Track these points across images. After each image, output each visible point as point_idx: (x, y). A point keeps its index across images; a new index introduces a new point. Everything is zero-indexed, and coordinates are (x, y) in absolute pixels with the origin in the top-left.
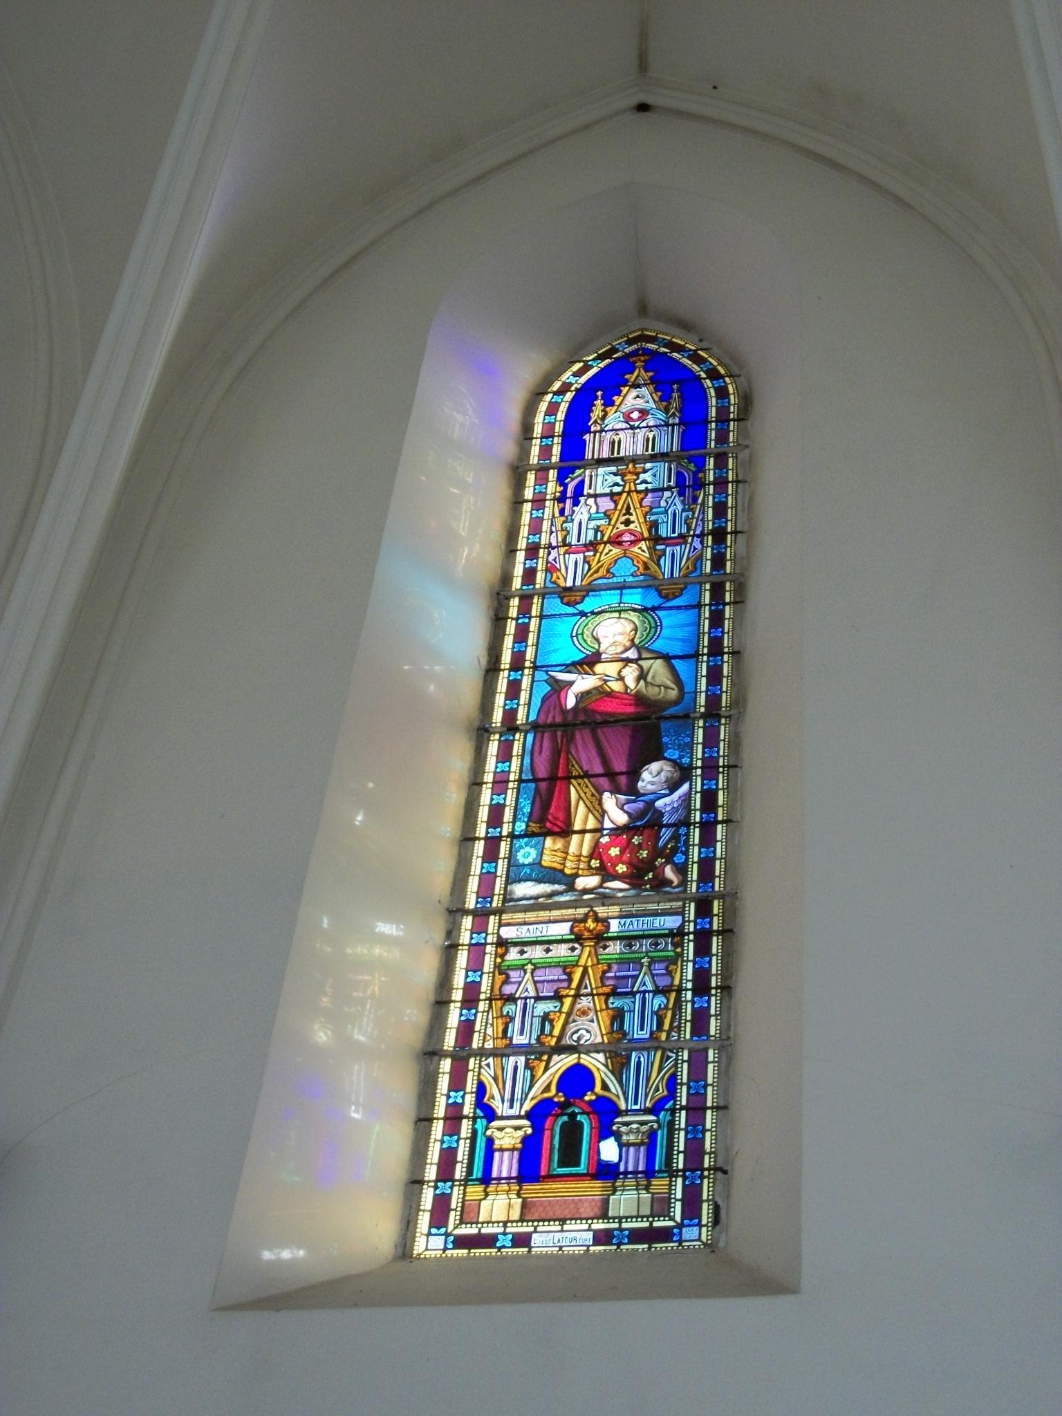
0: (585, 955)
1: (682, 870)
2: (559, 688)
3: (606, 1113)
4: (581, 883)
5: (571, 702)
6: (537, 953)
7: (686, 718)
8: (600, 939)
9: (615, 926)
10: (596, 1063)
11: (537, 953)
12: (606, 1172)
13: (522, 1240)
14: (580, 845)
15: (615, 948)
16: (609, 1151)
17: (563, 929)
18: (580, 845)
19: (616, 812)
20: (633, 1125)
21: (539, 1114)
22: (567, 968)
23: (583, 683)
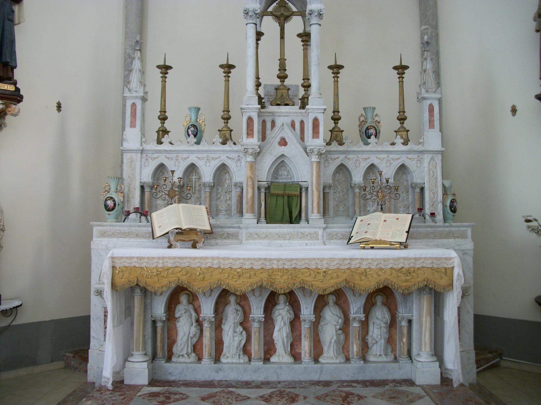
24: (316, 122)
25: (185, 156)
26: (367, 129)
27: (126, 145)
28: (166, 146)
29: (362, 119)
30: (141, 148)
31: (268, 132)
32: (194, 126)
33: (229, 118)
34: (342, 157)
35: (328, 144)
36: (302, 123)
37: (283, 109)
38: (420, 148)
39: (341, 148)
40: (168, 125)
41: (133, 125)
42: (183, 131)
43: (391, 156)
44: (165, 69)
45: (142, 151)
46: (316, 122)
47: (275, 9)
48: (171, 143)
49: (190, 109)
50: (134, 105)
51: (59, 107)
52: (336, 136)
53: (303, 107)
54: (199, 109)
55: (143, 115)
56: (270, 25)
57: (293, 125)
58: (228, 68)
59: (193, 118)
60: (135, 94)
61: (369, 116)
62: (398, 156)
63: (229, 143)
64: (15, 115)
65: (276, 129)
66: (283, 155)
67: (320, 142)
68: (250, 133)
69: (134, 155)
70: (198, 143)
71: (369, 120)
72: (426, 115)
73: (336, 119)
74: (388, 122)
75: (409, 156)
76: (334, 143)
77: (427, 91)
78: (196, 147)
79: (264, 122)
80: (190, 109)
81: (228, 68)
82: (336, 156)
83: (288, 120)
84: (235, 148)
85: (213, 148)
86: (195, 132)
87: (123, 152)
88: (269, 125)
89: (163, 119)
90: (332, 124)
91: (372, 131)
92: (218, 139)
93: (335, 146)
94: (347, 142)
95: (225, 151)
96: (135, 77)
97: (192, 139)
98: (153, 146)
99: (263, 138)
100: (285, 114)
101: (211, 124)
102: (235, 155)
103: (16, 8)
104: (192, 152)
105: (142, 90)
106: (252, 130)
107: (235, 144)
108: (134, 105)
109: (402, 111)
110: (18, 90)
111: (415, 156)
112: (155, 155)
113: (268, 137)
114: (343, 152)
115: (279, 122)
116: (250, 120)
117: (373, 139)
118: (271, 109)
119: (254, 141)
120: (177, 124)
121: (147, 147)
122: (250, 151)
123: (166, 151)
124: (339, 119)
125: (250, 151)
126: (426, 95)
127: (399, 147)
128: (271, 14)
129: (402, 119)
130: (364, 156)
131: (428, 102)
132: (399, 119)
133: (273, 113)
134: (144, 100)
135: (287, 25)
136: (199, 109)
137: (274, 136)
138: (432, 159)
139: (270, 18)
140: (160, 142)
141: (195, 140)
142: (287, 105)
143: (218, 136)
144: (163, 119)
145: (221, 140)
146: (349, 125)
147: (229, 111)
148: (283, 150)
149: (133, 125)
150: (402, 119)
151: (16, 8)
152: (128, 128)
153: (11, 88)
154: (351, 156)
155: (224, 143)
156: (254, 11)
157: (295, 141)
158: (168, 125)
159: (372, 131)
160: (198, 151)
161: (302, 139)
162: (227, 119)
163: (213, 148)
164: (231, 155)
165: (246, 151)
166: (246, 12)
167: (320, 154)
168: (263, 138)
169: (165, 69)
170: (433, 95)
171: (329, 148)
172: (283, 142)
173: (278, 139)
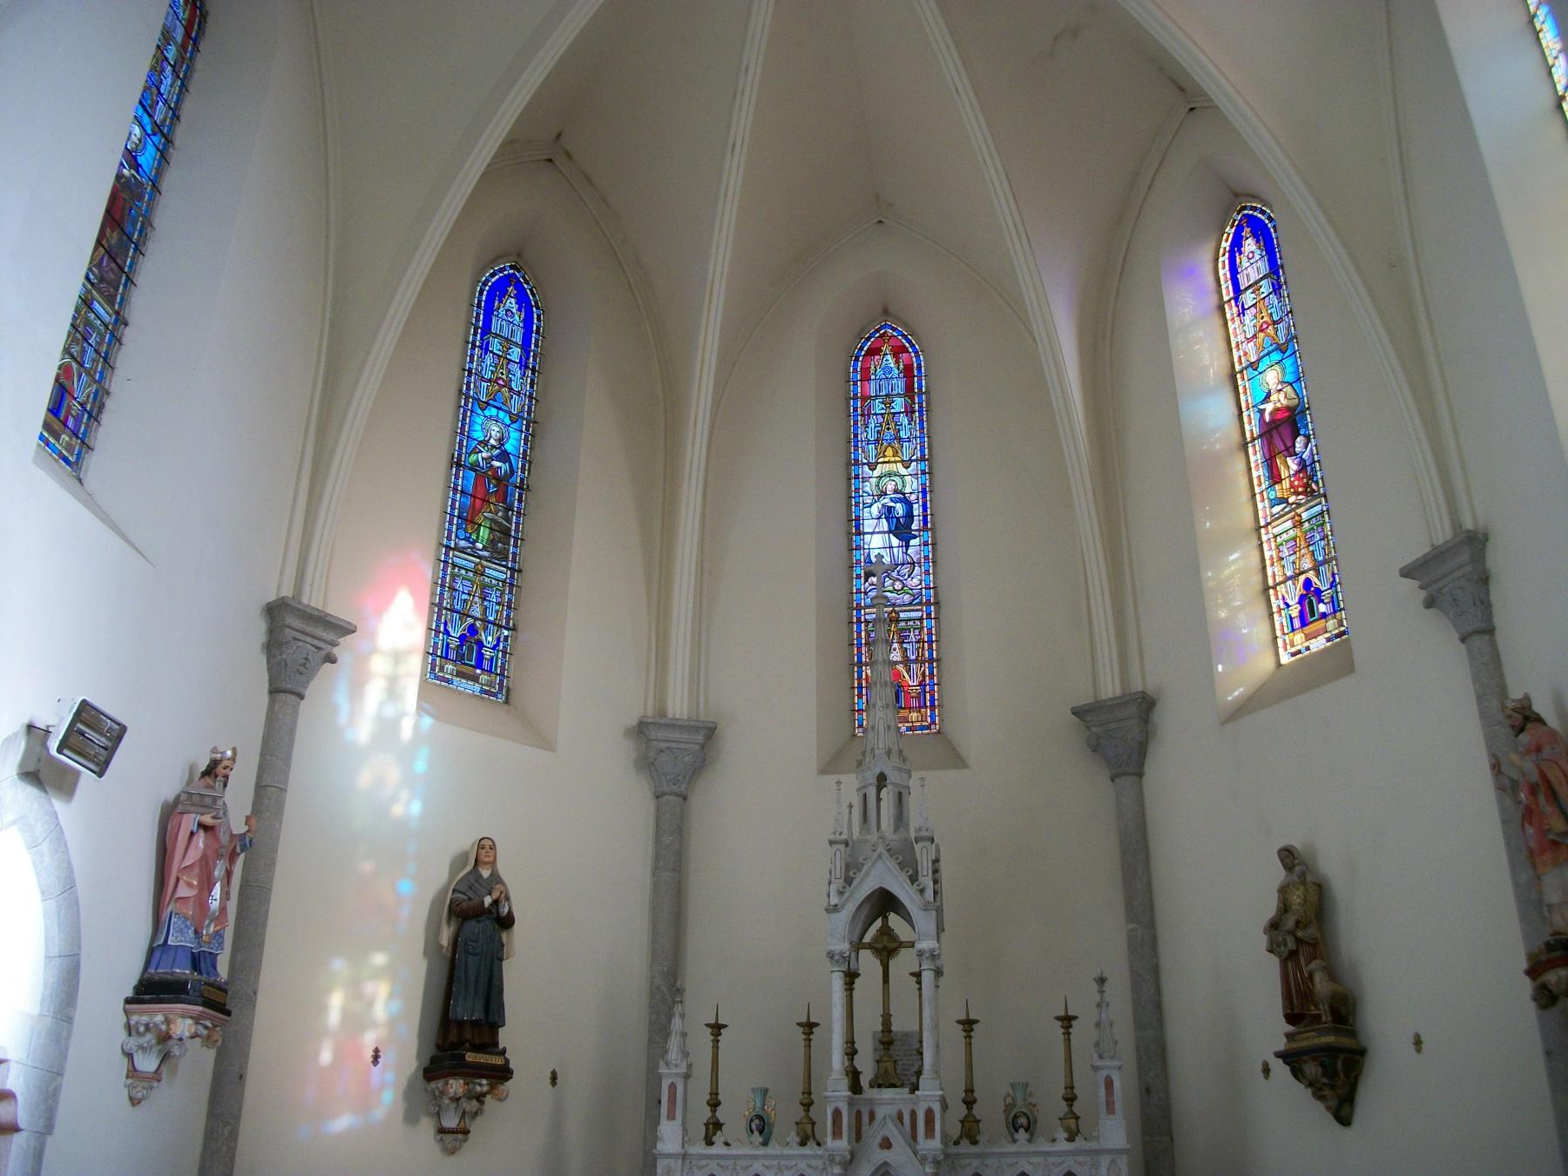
0: (1297, 532)
1: (1317, 483)
2: (1262, 412)
3: (1318, 592)
4: (1292, 499)
5: (1267, 419)
6: (1285, 536)
7: (1303, 412)
8: (1301, 523)
9: (1305, 516)
10: (1311, 575)
11: (1285, 536)
12: (1324, 616)
13: (1308, 649)
14: (1286, 484)
15: (1306, 525)
16: (1322, 608)
17: (1289, 524)
18: (1286, 484)
19: (1293, 465)
20: (1326, 596)
21: (1302, 599)
22: (1294, 539)
23: (1269, 407)
24: (929, 1114)
25: (745, 1164)
26: (1015, 1117)
27: (661, 1147)
28: (718, 1149)
29: (1009, 1100)
30: (681, 1151)
31: (865, 1128)
32: (760, 1117)
33: (811, 1103)
34: (976, 1162)
35: (956, 1143)
36: (913, 1114)
37: (888, 1094)
38: (1093, 1145)
39: (974, 1149)
40: (721, 1114)
41: (671, 1117)
42: (743, 1123)
43: (1050, 1159)
44: (717, 1028)
45: (685, 1156)
46: (929, 1114)
47: (875, 939)
48: (727, 1144)
49: (753, 1090)
50: (673, 1087)
51: (554, 1078)
52: (970, 1130)
53: (915, 1088)
54: (766, 1091)
55: (685, 1100)
56: (868, 963)
57: (900, 1117)
58: (809, 1027)
59: (758, 1104)
60: (674, 1070)
61: (1019, 1096)
62: (1060, 1160)
63: (811, 1143)
64: (500, 1100)
65: (876, 1124)
66: (886, 1164)
67: (935, 1144)
68: (837, 1134)
69: (672, 1163)
70: (765, 1144)
71: (1020, 1102)
72: (1102, 1092)
73: (969, 1103)
74: (1051, 1107)
75: (1080, 1159)
76: (965, 1142)
77: (1101, 1057)
78: (761, 1151)
79: (859, 1115)
80: (753, 1090)
81: (809, 1027)
82: (967, 1161)
83: (892, 1110)
84: (820, 1151)
85: (787, 1151)
86: (762, 1126)
87: (655, 1159)
88: (865, 1118)
89: (714, 1104)
90: (962, 1110)
91: (1023, 1120)
92: (794, 1138)
93: (965, 1147)
94: (982, 1138)
95: (804, 1156)
96: (674, 1044)
97: (757, 1138)
98: (699, 1148)
99: (858, 1137)
100: (889, 1100)
101: (785, 1115)
102: (819, 1163)
103: (504, 936)
104: (755, 1157)
105: (684, 1065)
106: (840, 1128)
107: (819, 1144)
108: (673, 1087)
109: (1070, 1087)
110: (507, 1061)
111: (1087, 1159)
112: (704, 1162)
113: (864, 1135)
114: (978, 1156)
115: (880, 1113)
116: (837, 1114)
117: (1022, 1135)
118: (870, 1093)
119: (842, 1145)
120: (734, 1113)
121: (692, 1150)
122: (838, 1159)
123: (718, 1157)
124: (975, 1101)
125: (838, 1159)
126: (1099, 1063)
127: (1063, 1145)
128: (870, 946)
129: (1070, 1099)
130: (1010, 1160)
131: (1105, 1073)
132: (1066, 1100)
133: (871, 1101)
134: (687, 1077)
135: (892, 963)
136: (766, 1091)
137: (873, 1135)
138: (1113, 1162)
139: (868, 952)
140: (709, 1142)
141: (761, 1139)
142: (893, 1086)
143: (793, 1133)
144: (714, 1104)
145: (798, 1139)
146: (990, 1111)
147: (810, 1093)
148: (885, 1155)
149: (671, 1117)
150: (1070, 1099)
151: (504, 936)
152: (663, 1121)
153: (498, 1061)
154: (989, 1161)
155: (803, 1144)
156: (841, 954)
157: (902, 1142)
158: (721, 1114)
159: (1023, 1120)
160: (765, 1157)
161: (914, 1137)
162: (807, 1105)
163: (787, 1151)
164: (813, 1163)
165: (831, 1159)
166: (831, 955)
167: (937, 1163)
168: (858, 1137)
169: (717, 1028)
170: (1109, 1063)
171: (953, 1150)
172: (886, 1144)
173: (878, 1139)
